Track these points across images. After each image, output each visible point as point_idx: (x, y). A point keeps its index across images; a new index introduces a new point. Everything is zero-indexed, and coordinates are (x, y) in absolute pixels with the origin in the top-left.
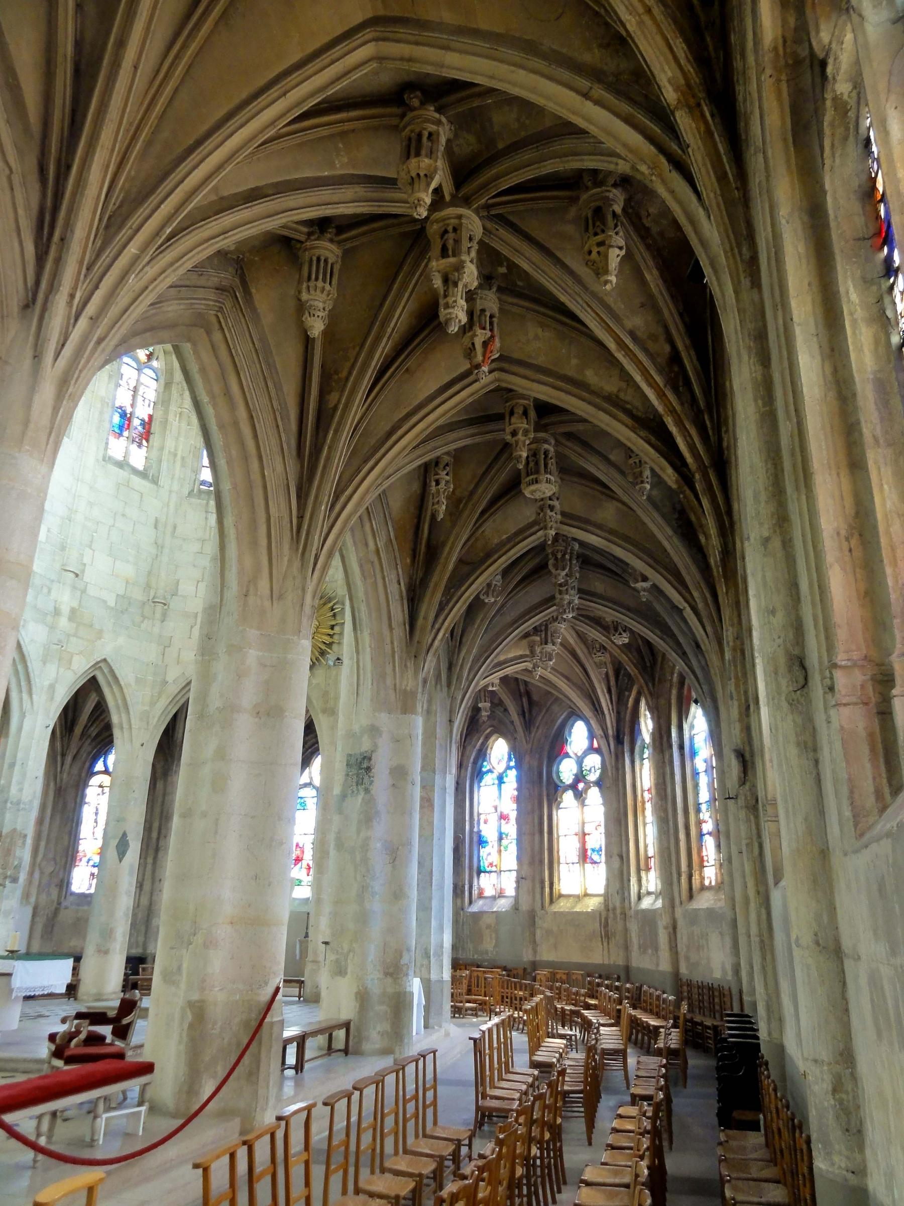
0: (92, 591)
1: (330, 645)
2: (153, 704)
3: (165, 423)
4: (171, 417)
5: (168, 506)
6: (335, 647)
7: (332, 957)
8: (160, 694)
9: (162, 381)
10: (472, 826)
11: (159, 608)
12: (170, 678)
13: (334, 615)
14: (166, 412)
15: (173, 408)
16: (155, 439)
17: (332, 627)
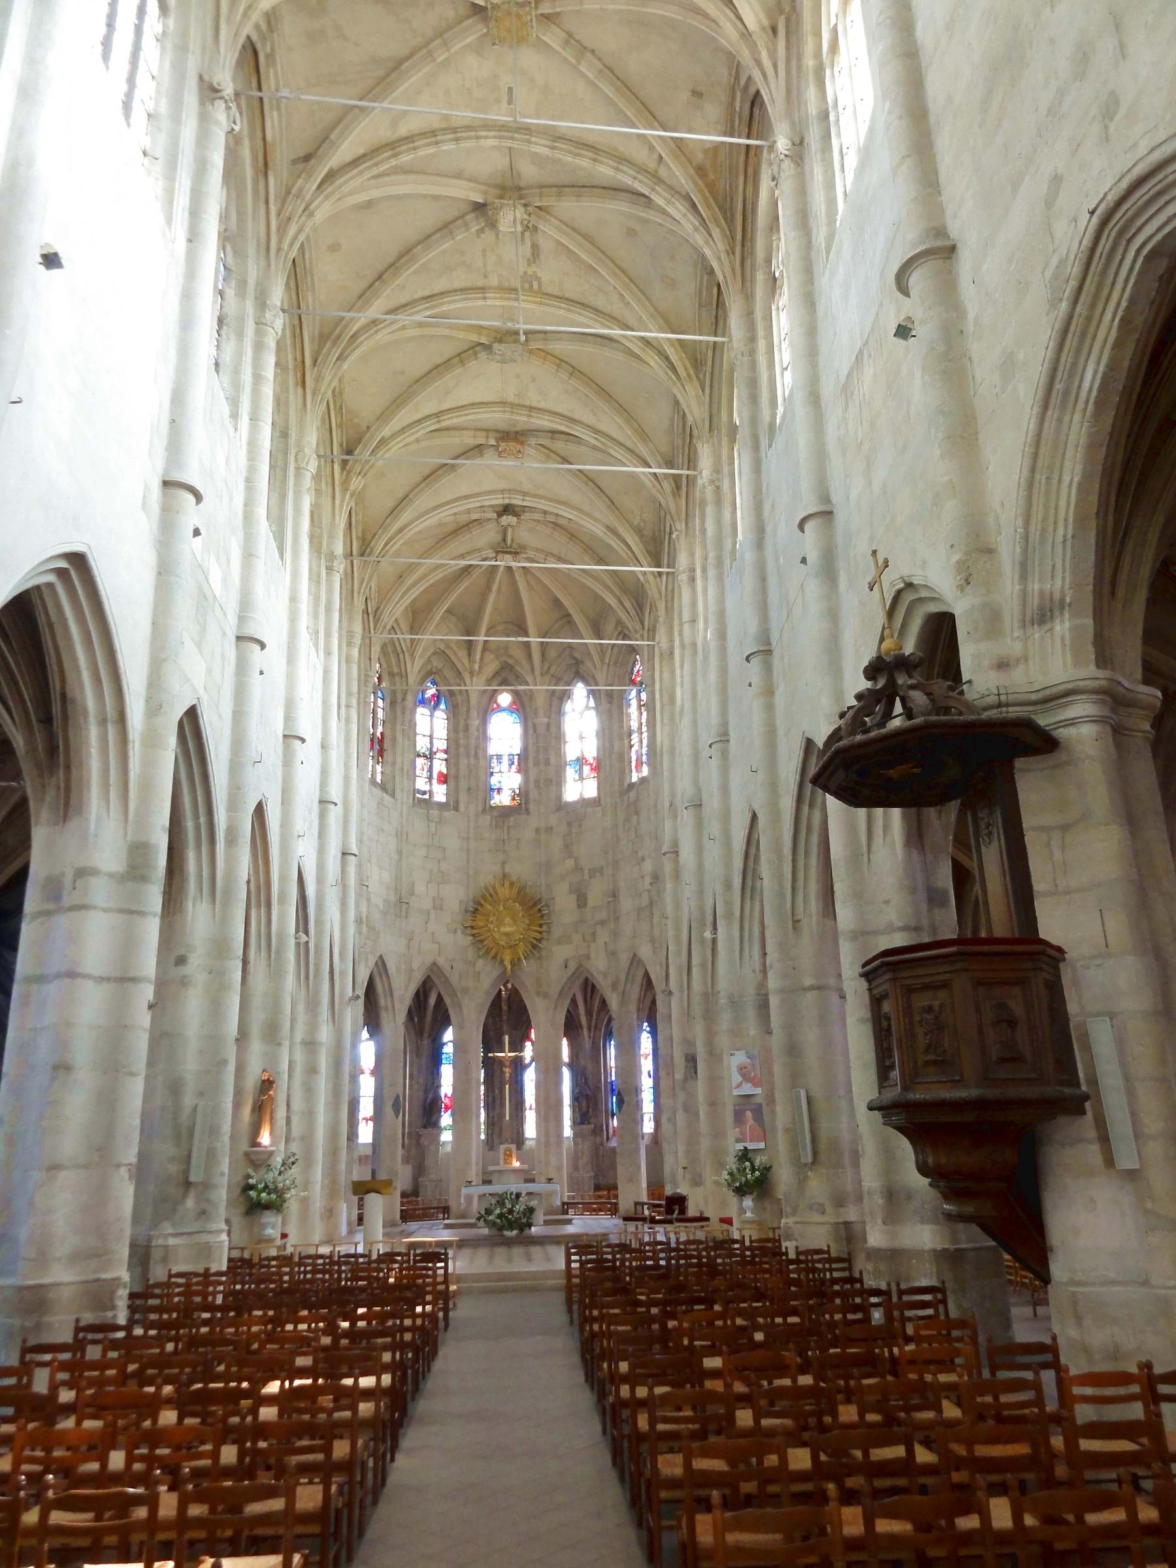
0: (374, 899)
1: (539, 940)
2: (407, 987)
3: (394, 739)
4: (399, 736)
5: (402, 815)
6: (544, 942)
7: (688, 1176)
8: (410, 979)
9: (388, 700)
10: (606, 1078)
11: (404, 906)
12: (415, 965)
13: (542, 916)
14: (394, 730)
15: (399, 727)
16: (388, 755)
17: (541, 926)
